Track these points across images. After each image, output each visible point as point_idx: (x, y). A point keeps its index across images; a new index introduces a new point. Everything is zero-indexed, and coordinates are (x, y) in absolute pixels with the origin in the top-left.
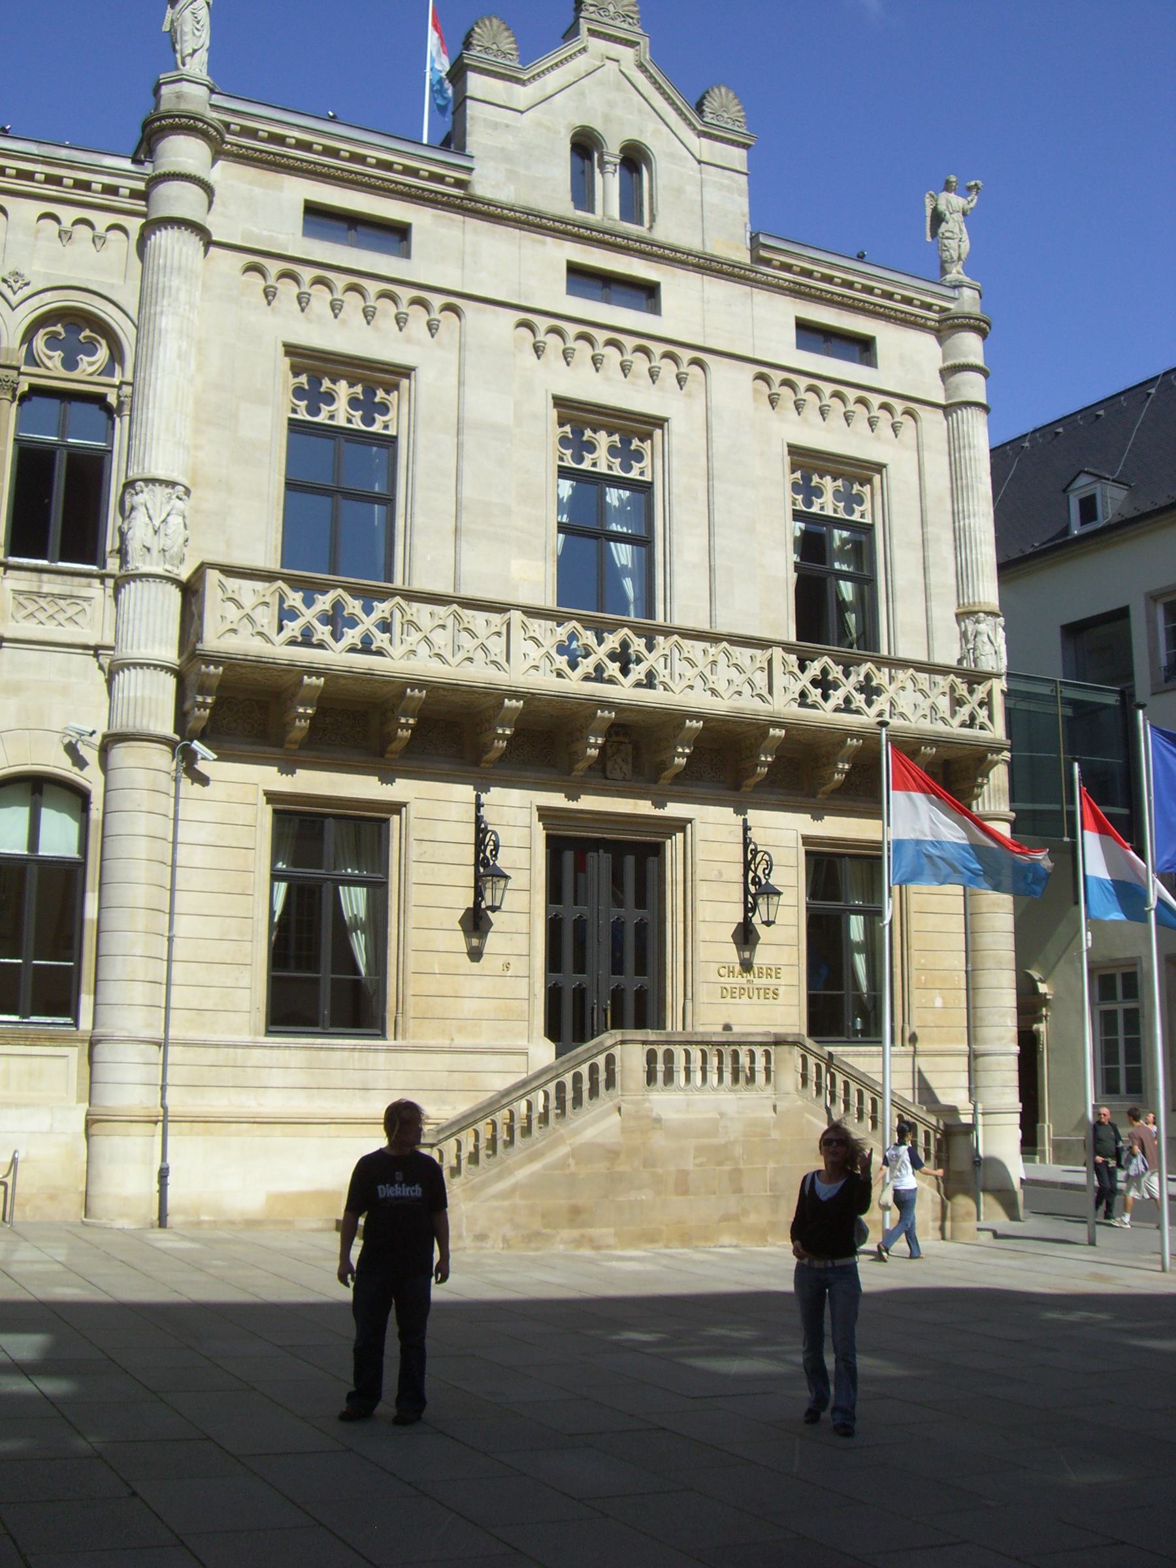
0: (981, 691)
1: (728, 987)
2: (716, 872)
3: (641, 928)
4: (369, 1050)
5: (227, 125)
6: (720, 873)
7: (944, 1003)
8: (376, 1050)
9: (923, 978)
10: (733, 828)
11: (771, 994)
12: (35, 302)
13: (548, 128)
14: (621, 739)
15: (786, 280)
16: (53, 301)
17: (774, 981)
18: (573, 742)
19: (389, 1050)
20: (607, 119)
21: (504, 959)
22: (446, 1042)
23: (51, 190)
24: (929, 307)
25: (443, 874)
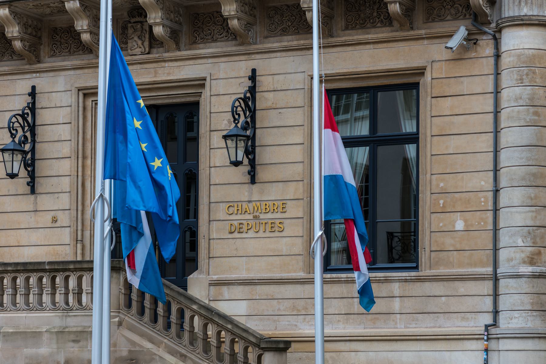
7: (466, 225)
9: (441, 202)
10: (242, 80)
17: (279, 215)
21: (52, 214)
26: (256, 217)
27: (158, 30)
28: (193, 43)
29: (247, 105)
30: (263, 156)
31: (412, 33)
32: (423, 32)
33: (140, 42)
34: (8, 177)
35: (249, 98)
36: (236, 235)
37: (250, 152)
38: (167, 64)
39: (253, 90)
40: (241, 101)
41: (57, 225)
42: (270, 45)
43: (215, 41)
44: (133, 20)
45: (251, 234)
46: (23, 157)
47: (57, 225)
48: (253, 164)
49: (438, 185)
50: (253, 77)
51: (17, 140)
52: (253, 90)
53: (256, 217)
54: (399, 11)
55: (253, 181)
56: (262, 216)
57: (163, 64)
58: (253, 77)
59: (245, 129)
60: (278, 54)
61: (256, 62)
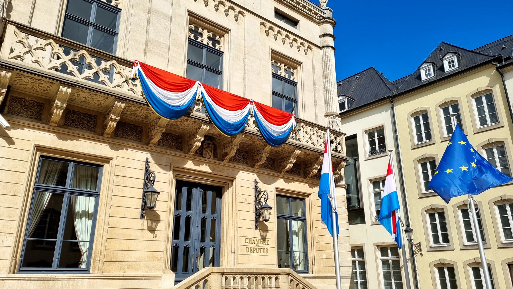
0: (339, 139)
1: (249, 247)
2: (244, 199)
3: (213, 221)
4: (78, 279)
6: (246, 200)
7: (326, 256)
8: (83, 279)
9: (319, 246)
10: (251, 182)
11: (265, 251)
14: (210, 142)
18: (190, 140)
19: (90, 279)
22: (122, 274)
24: (316, 14)
25: (127, 192)
26: (257, 246)
34: (148, 209)
36: (249, 253)
41: (156, 239)
45: (255, 253)
47: (156, 239)
49: (317, 240)
53: (257, 246)
56: (260, 245)
60: (265, 175)
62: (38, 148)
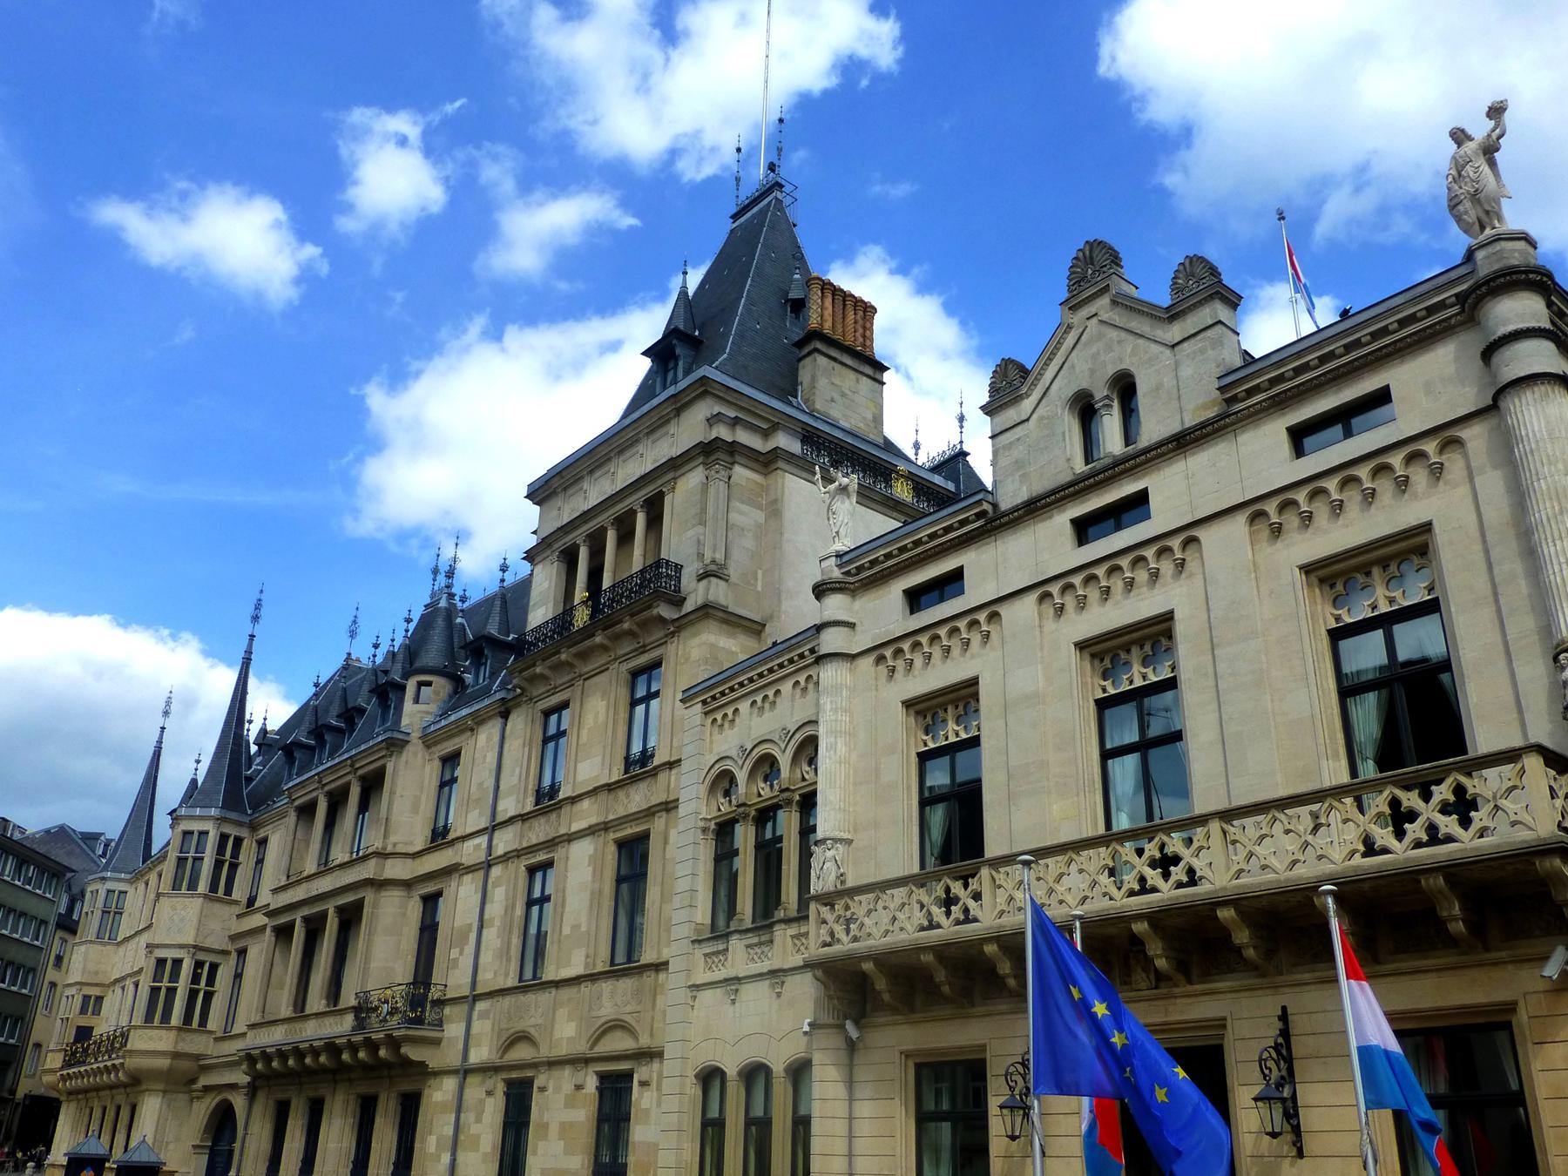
5: (848, 573)
12: (793, 742)
13: (1047, 418)
15: (1260, 402)
16: (799, 737)
20: (1092, 371)
23: (792, 668)
24: (1442, 305)
27: (1161, 963)
28: (1206, 976)
29: (1278, 1053)
30: (1308, 1120)
31: (1487, 955)
32: (1504, 954)
33: (1144, 975)
35: (1281, 1044)
37: (1291, 1113)
38: (1178, 1001)
39: (1285, 1033)
40: (1271, 1050)
42: (1298, 977)
43: (1233, 971)
44: (1134, 949)
46: (1025, 1113)
48: (1297, 1130)
50: (1284, 1017)
51: (1017, 1092)
52: (1285, 1033)
54: (1464, 930)
55: (1300, 1154)
57: (1173, 1000)
58: (1284, 1017)
59: (1279, 1086)
61: (1287, 998)
62: (907, 1055)
